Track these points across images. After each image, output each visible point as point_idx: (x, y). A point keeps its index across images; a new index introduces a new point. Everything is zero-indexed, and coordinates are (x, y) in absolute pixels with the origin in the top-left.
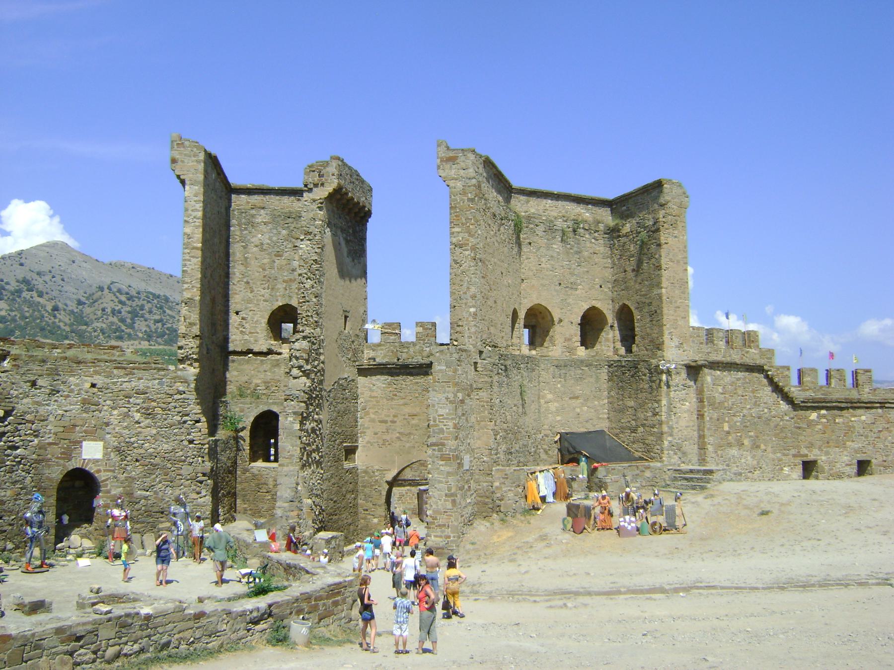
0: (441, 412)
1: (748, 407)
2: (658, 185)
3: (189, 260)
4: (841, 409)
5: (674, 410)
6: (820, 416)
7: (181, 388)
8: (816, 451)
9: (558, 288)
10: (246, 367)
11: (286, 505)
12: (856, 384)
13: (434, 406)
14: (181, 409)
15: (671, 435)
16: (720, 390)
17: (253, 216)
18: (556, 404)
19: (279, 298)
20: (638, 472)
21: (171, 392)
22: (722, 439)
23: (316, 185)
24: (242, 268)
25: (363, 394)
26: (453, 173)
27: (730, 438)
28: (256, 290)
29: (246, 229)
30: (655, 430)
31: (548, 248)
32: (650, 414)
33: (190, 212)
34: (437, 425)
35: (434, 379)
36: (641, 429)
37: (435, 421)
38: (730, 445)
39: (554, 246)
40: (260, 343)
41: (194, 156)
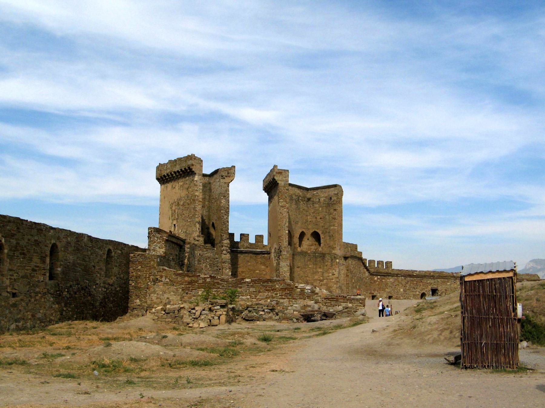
0: (285, 269)
4: (384, 276)
6: (378, 279)
8: (376, 292)
12: (387, 267)
23: (226, 177)
32: (330, 274)
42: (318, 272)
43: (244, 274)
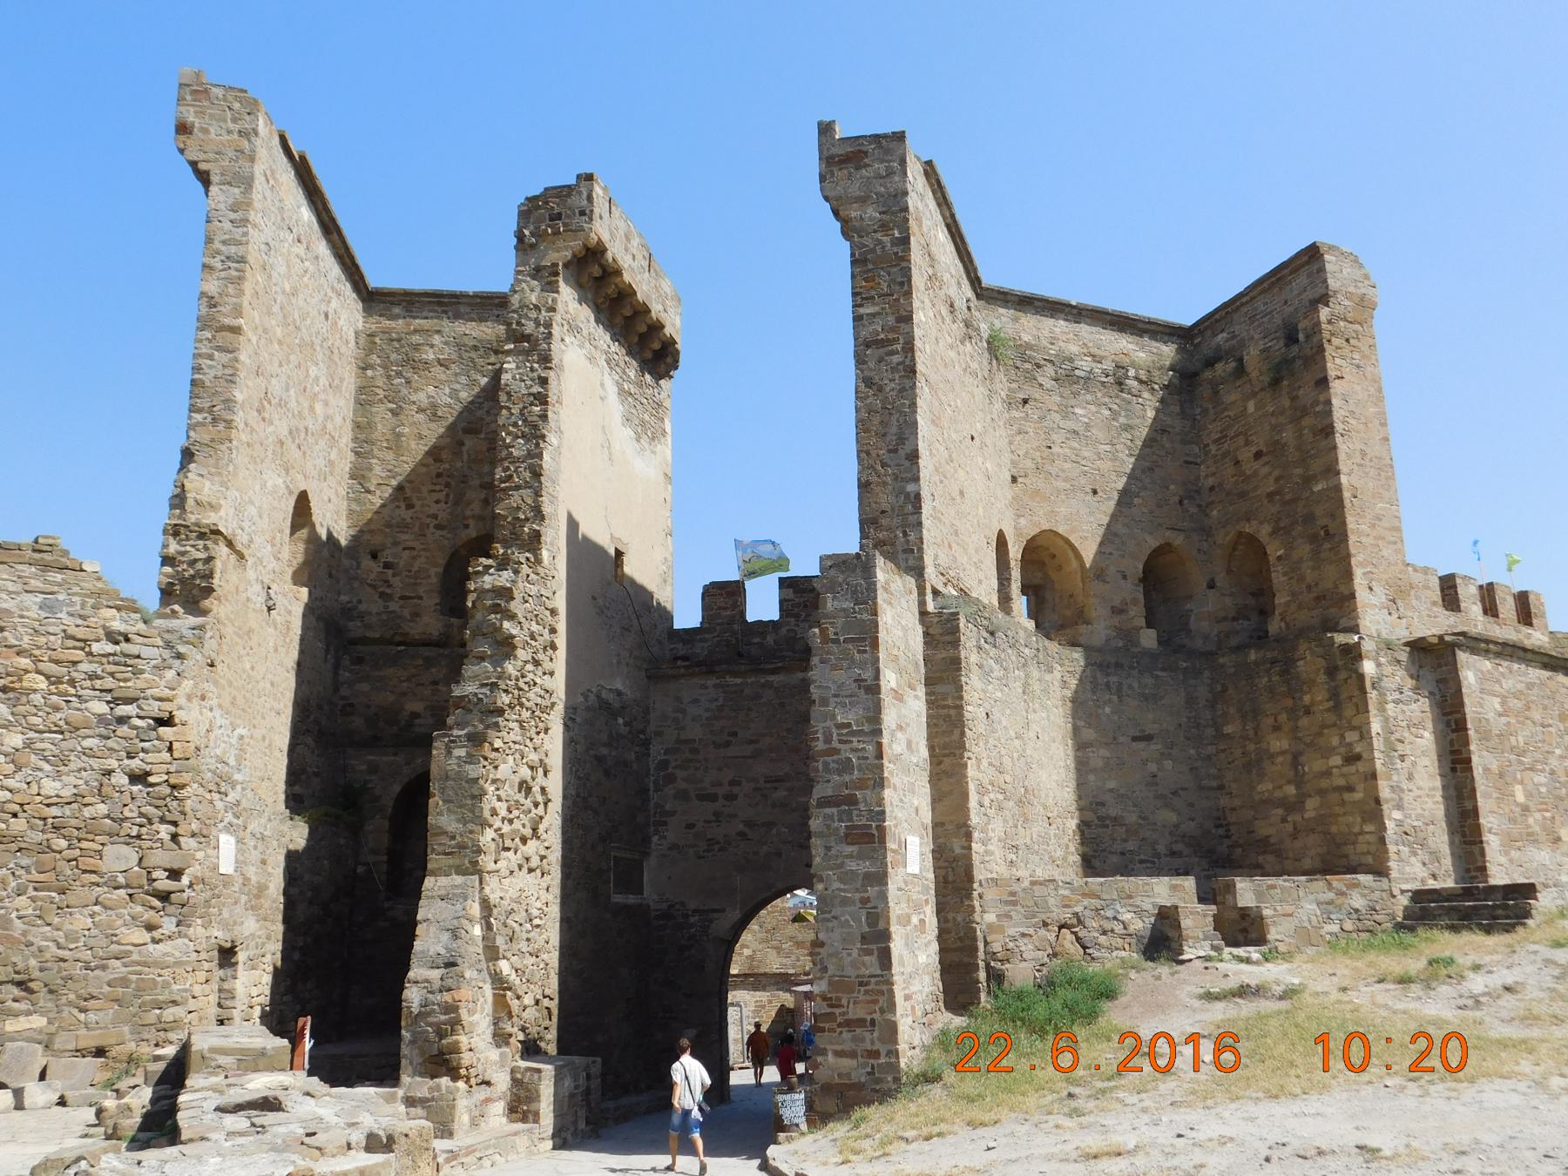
1: (1558, 752)
2: (1312, 255)
3: (211, 357)
5: (1399, 746)
7: (117, 625)
9: (1089, 497)
10: (390, 671)
11: (435, 974)
13: (825, 702)
14: (109, 683)
15: (1399, 807)
16: (1498, 707)
17: (416, 347)
18: (1104, 752)
19: (471, 522)
20: (1331, 895)
21: (81, 633)
22: (1512, 820)
24: (390, 456)
25: (659, 734)
26: (855, 189)
27: (1531, 821)
28: (418, 503)
29: (399, 374)
30: (1358, 796)
31: (1066, 412)
32: (1336, 760)
33: (217, 245)
34: (837, 751)
35: (823, 631)
36: (1312, 804)
37: (828, 740)
38: (1532, 839)
39: (1077, 410)
40: (426, 619)
41: (234, 120)
42: (1272, 756)
43: (781, 794)
